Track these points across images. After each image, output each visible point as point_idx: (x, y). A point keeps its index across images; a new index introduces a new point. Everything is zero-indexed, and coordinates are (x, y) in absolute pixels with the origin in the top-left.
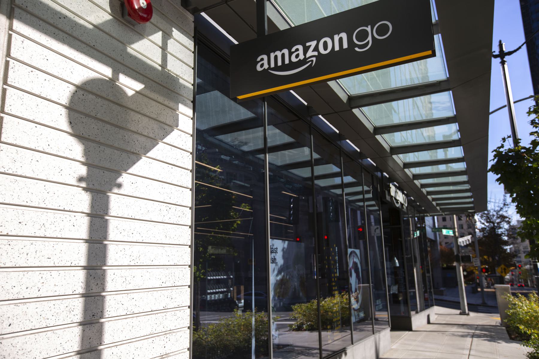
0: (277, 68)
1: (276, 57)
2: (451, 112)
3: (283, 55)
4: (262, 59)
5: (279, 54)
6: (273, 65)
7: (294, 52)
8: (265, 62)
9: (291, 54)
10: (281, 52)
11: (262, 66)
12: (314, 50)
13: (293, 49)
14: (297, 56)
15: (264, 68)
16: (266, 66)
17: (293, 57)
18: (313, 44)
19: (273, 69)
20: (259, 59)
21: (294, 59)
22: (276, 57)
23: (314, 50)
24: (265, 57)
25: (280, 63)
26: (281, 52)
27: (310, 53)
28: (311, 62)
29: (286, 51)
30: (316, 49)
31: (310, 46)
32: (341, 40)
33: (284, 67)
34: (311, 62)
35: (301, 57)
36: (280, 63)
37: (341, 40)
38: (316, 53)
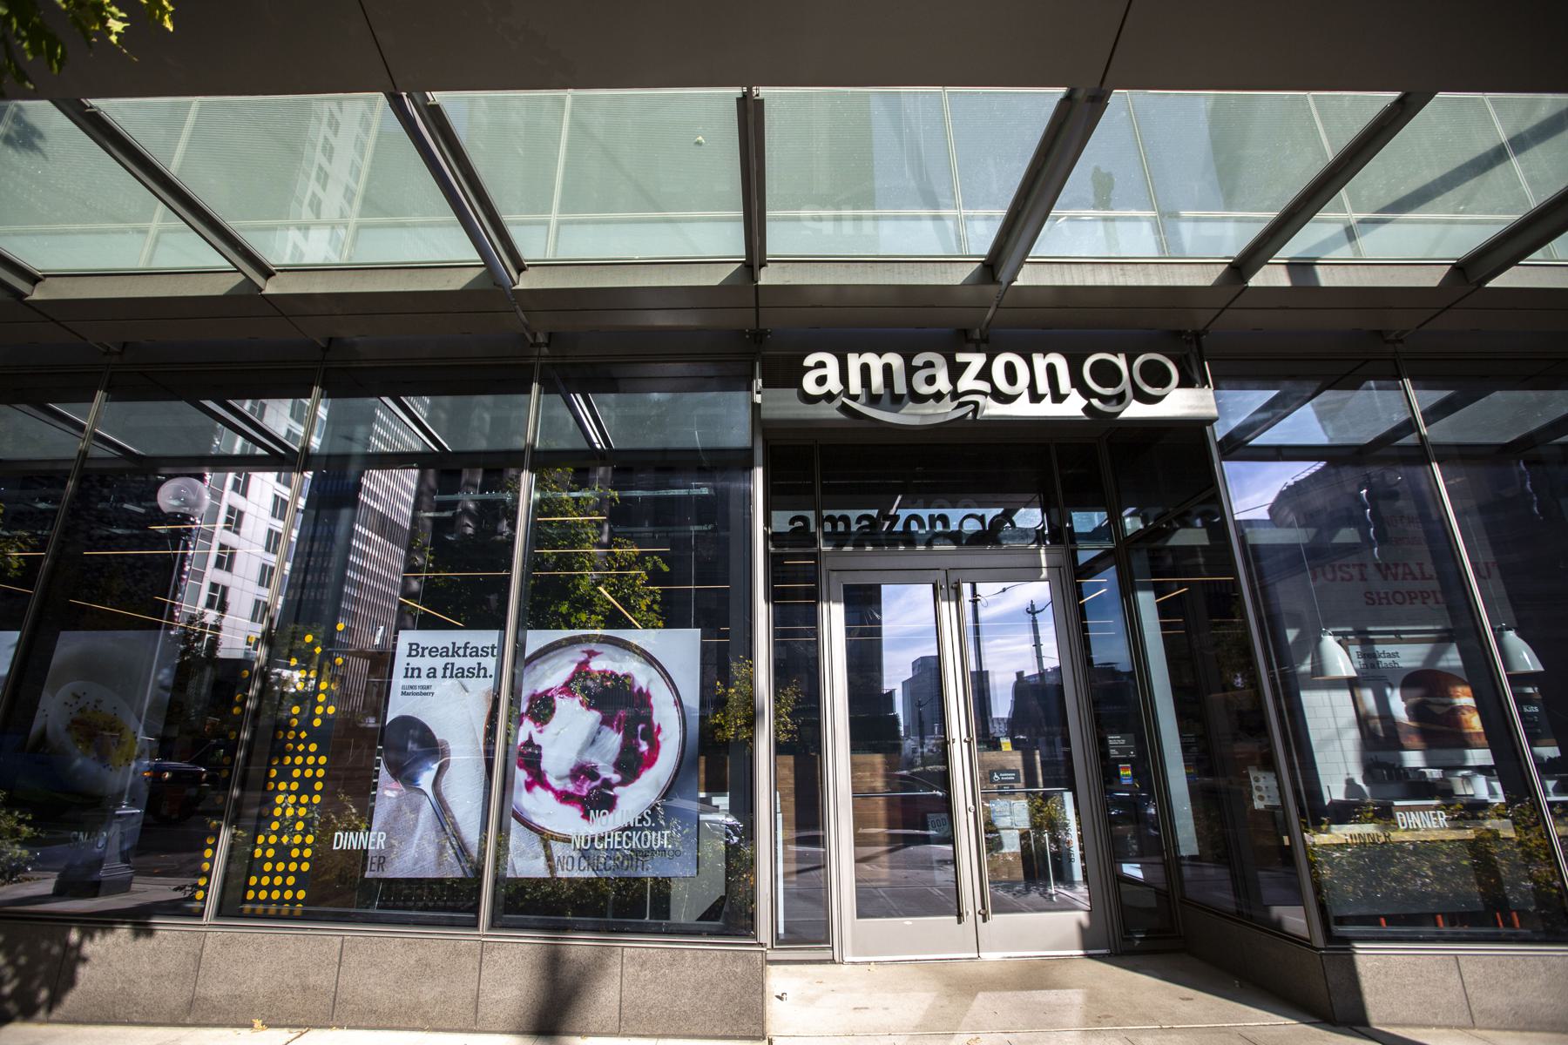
1: (865, 369)
2: (947, 603)
3: (887, 369)
5: (875, 362)
7: (919, 368)
9: (910, 371)
10: (880, 356)
11: (821, 381)
12: (979, 377)
13: (918, 360)
15: (829, 391)
18: (977, 361)
20: (810, 361)
22: (865, 369)
23: (979, 377)
24: (831, 361)
26: (880, 356)
27: (967, 382)
28: (972, 406)
29: (895, 360)
30: (985, 374)
32: (1051, 370)
34: (972, 406)
37: (1051, 370)
38: (984, 386)
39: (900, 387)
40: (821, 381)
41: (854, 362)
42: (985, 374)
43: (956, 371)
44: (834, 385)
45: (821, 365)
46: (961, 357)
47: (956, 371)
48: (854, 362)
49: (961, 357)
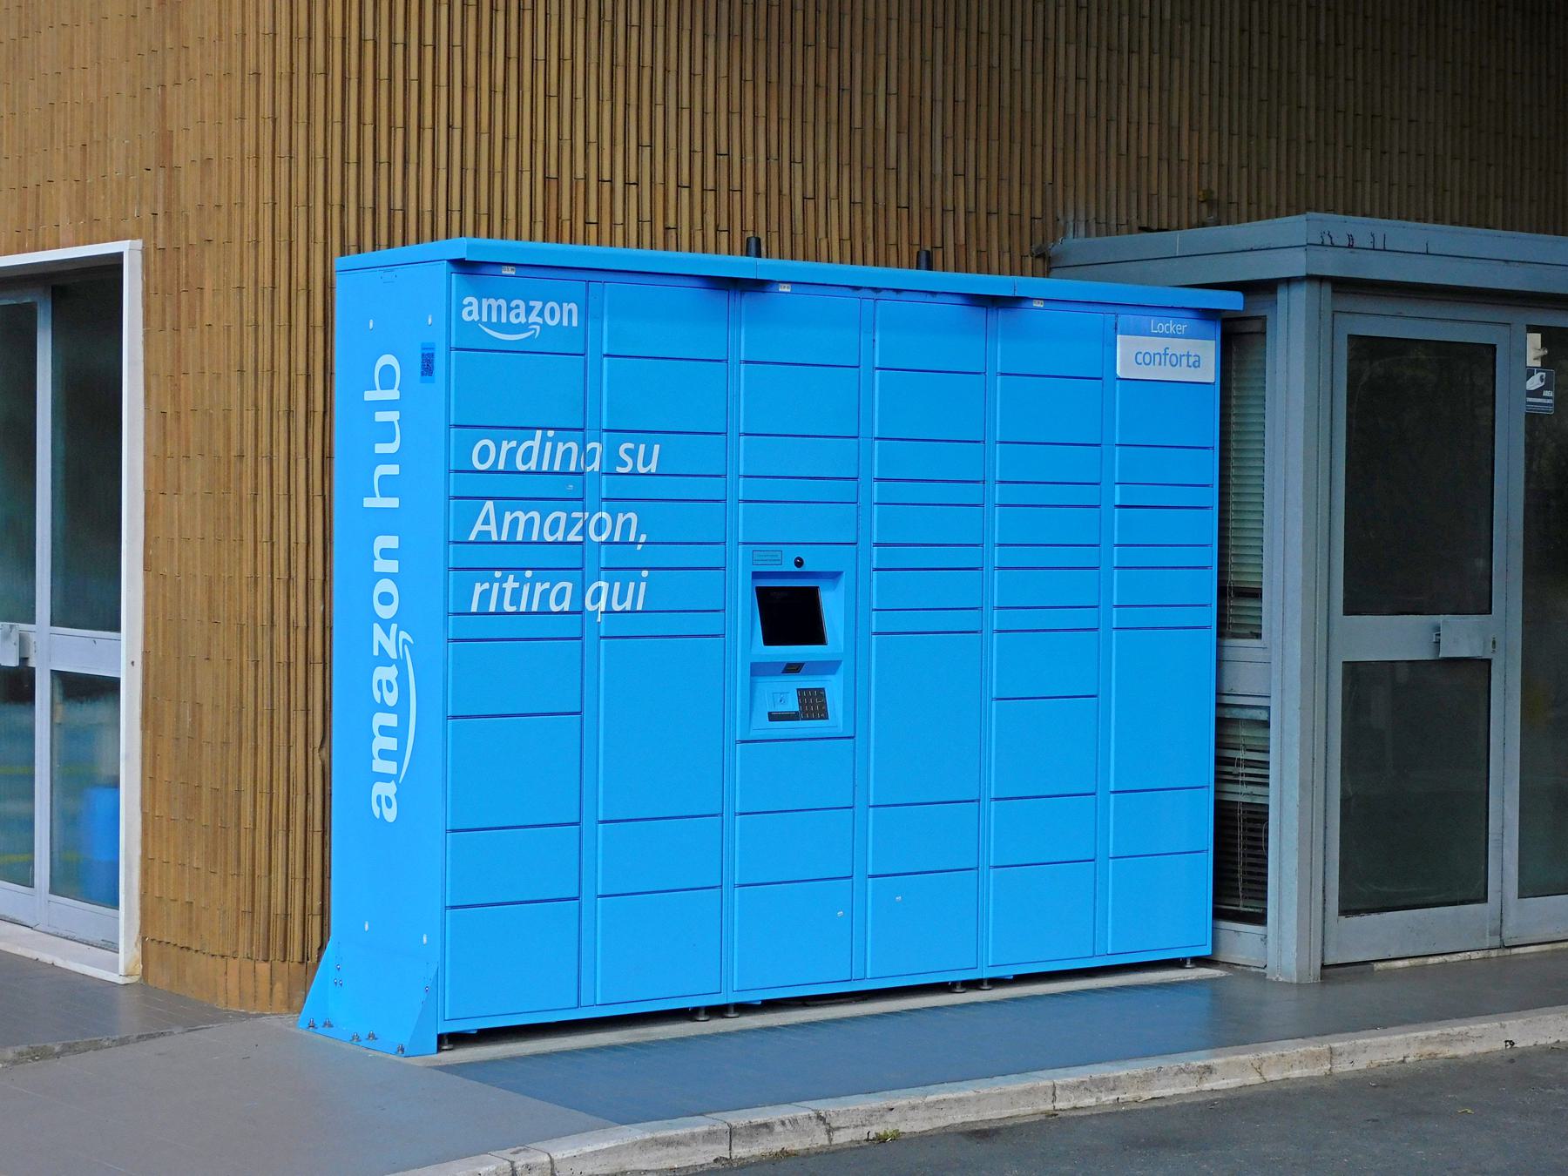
0: (489, 324)
3: (499, 308)
4: (470, 304)
6: (485, 319)
7: (513, 309)
8: (475, 308)
9: (509, 309)
11: (470, 313)
13: (513, 304)
14: (517, 316)
16: (475, 317)
17: (513, 314)
18: (538, 305)
19: (484, 324)
20: (466, 301)
21: (514, 320)
22: (490, 307)
25: (494, 319)
27: (533, 318)
28: (533, 332)
29: (502, 302)
30: (541, 314)
31: (534, 307)
32: (570, 312)
33: (498, 327)
34: (533, 332)
35: (522, 319)
36: (494, 319)
37: (570, 312)
38: (540, 320)
39: (504, 320)
40: (470, 313)
41: (485, 303)
42: (541, 314)
43: (529, 310)
44: (475, 317)
45: (470, 304)
46: (532, 303)
47: (529, 310)
48: (485, 303)
49: (532, 303)
